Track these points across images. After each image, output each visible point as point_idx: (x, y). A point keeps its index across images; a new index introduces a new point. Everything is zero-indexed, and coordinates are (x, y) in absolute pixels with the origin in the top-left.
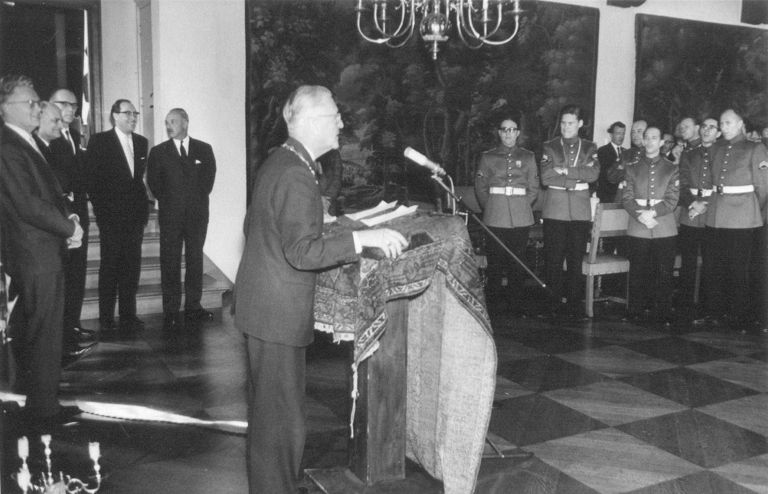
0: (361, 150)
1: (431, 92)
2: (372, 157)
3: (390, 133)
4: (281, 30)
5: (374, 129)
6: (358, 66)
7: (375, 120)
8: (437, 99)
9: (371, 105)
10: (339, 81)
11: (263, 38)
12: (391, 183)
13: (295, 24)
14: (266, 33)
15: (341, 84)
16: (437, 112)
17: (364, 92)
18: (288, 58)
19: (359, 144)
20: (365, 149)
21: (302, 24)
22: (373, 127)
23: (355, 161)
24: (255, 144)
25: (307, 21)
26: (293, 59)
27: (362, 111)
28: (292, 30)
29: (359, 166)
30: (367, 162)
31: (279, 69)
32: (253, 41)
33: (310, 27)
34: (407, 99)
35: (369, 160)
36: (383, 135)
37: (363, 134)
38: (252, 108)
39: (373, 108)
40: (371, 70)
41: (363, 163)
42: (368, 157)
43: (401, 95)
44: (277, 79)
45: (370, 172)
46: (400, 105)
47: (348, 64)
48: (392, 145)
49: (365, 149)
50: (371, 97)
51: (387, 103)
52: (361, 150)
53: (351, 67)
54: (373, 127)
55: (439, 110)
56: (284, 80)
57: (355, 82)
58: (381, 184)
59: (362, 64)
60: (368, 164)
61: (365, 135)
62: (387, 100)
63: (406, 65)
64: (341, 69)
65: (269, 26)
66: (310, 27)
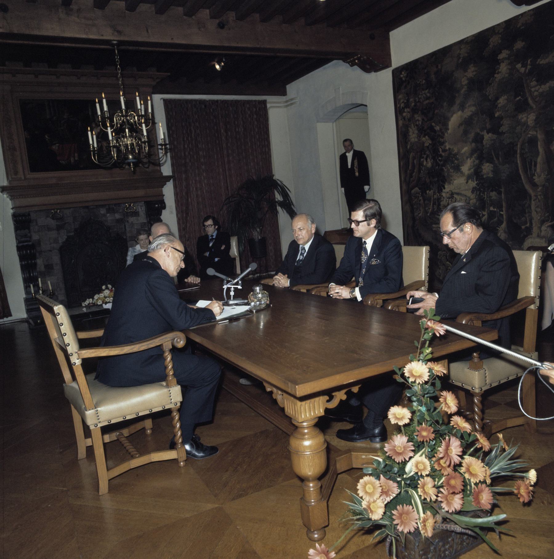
0: (467, 182)
1: (523, 117)
2: (476, 187)
3: (488, 164)
4: (413, 104)
5: (475, 163)
6: (460, 113)
7: (475, 155)
8: (529, 123)
9: (473, 141)
10: (448, 129)
11: (404, 114)
12: (492, 209)
13: (420, 96)
14: (406, 110)
15: (449, 131)
16: (529, 136)
17: (466, 133)
18: (417, 123)
19: (465, 178)
20: (470, 181)
21: (424, 95)
22: (474, 161)
23: (463, 192)
24: (404, 187)
25: (427, 91)
26: (420, 123)
27: (465, 149)
28: (419, 101)
29: (466, 196)
30: (473, 192)
31: (413, 133)
32: (400, 118)
33: (428, 95)
34: (500, 130)
35: (474, 190)
36: (482, 167)
37: (467, 169)
38: (402, 163)
39: (473, 144)
40: (469, 113)
41: (469, 194)
42: (473, 188)
43: (495, 129)
44: (413, 140)
45: (475, 201)
46: (495, 137)
47: (454, 113)
48: (491, 175)
49: (470, 181)
50: (472, 136)
51: (483, 138)
52: (467, 182)
53: (455, 116)
54: (474, 161)
55: (532, 133)
56: (416, 140)
57: (459, 127)
58: (485, 211)
59: (463, 111)
60: (473, 193)
61: (469, 170)
62: (483, 136)
63: (497, 98)
64: (448, 119)
65: (407, 105)
66: (428, 95)
